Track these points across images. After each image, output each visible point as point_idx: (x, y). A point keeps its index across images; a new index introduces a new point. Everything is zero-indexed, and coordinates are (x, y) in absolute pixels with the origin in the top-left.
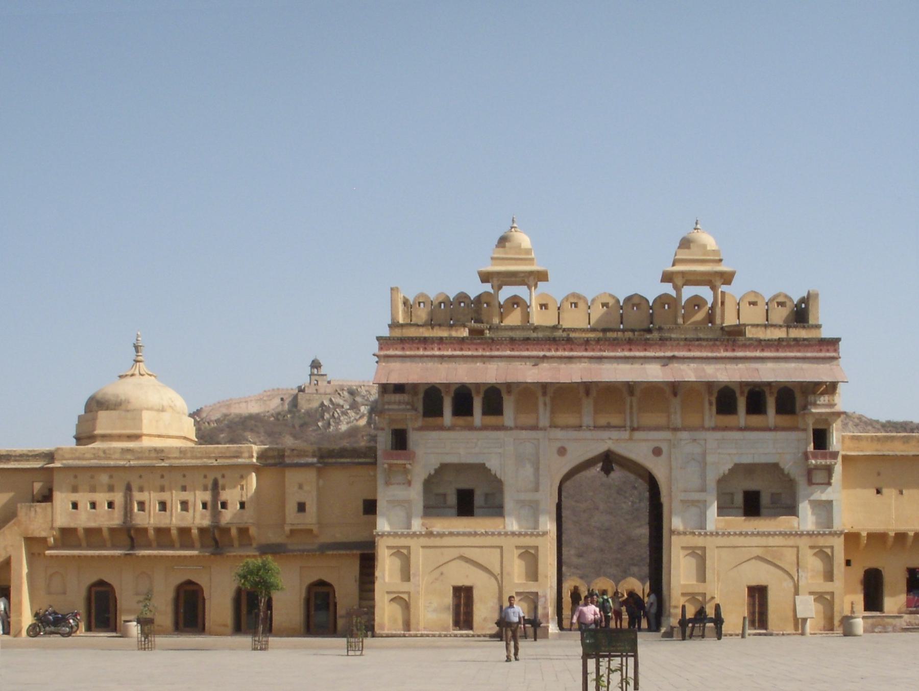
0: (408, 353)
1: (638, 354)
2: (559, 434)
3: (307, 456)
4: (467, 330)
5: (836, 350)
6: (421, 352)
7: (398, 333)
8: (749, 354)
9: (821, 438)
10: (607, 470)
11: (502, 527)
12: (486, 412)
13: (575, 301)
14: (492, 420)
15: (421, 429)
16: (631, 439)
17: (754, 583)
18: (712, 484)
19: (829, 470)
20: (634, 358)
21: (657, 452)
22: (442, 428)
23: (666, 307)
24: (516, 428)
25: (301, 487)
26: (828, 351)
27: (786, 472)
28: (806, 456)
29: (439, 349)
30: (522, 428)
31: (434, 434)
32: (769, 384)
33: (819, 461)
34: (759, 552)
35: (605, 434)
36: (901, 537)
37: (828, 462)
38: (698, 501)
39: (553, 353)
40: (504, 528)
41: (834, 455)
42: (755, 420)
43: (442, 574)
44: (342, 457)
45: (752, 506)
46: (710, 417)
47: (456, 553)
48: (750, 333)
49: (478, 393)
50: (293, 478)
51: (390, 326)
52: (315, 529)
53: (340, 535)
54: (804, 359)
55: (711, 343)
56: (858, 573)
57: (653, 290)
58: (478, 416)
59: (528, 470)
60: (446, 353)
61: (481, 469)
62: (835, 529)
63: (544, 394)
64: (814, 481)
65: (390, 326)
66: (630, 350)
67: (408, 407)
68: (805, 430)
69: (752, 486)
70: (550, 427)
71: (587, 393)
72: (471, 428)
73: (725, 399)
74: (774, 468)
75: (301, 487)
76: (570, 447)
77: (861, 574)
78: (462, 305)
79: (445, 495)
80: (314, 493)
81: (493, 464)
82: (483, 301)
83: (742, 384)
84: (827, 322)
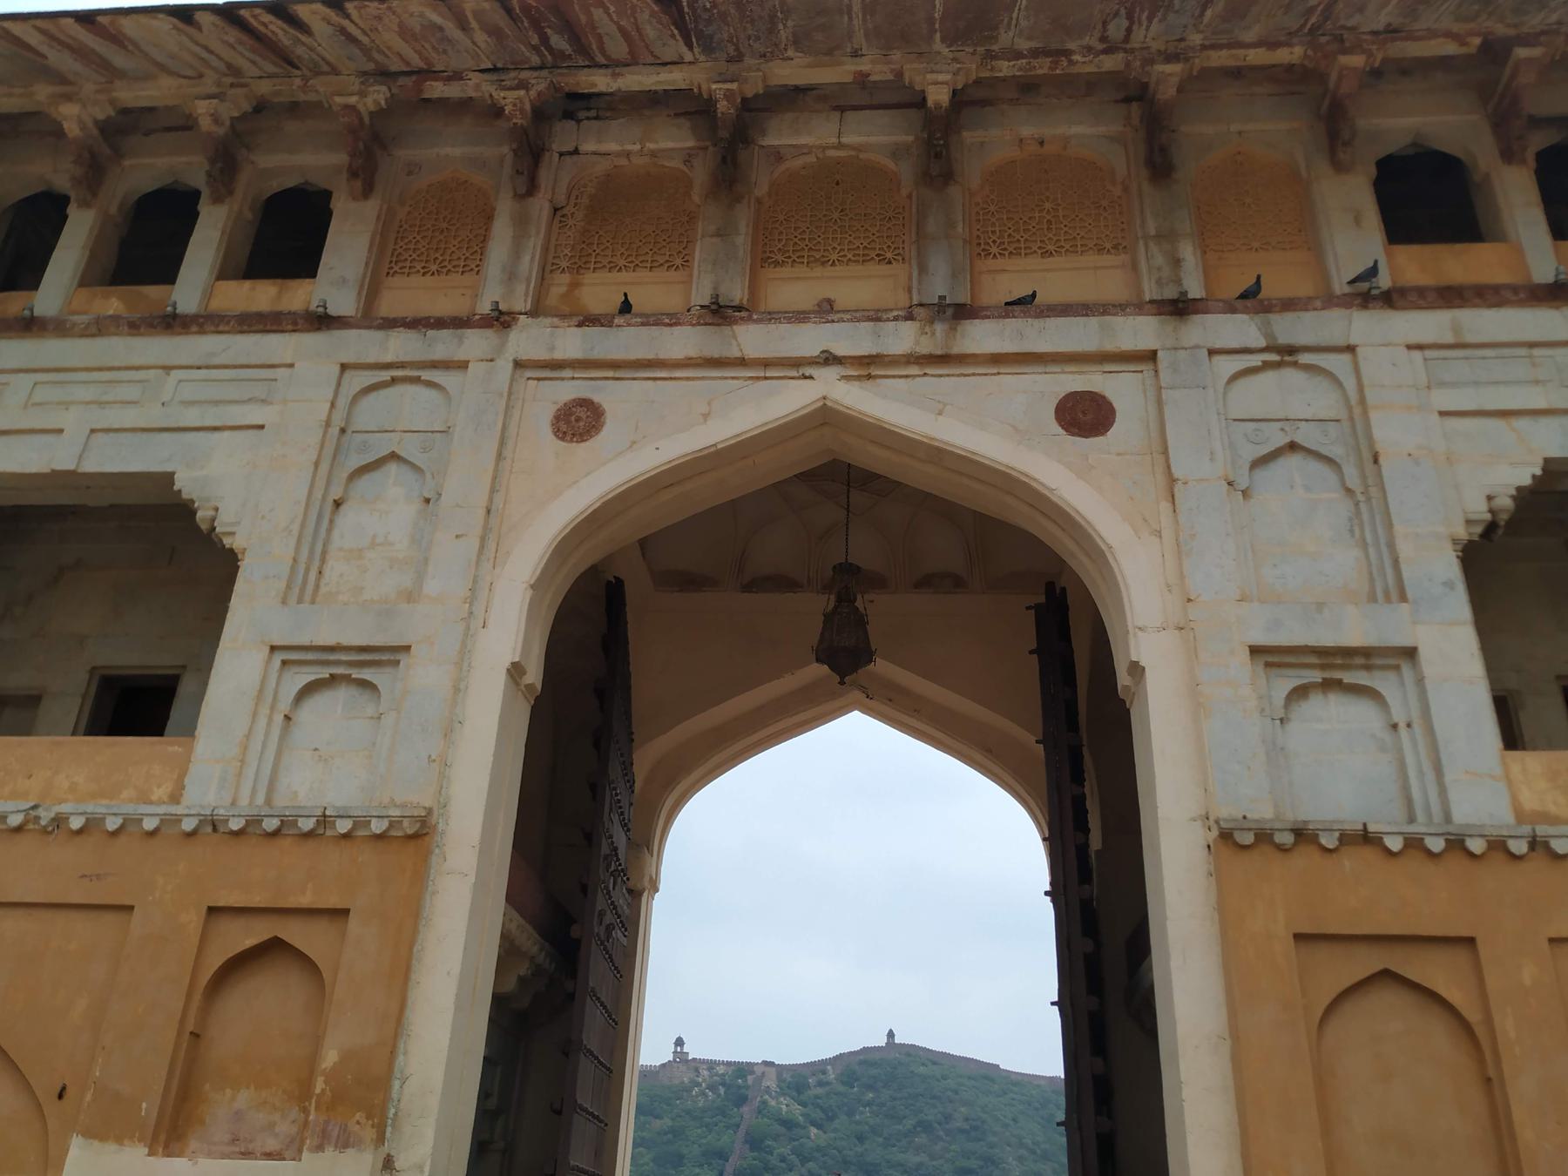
11: (160, 793)
21: (1085, 416)
38: (1365, 656)
40: (175, 798)
58: (191, 286)
70: (534, 313)
76: (613, 396)
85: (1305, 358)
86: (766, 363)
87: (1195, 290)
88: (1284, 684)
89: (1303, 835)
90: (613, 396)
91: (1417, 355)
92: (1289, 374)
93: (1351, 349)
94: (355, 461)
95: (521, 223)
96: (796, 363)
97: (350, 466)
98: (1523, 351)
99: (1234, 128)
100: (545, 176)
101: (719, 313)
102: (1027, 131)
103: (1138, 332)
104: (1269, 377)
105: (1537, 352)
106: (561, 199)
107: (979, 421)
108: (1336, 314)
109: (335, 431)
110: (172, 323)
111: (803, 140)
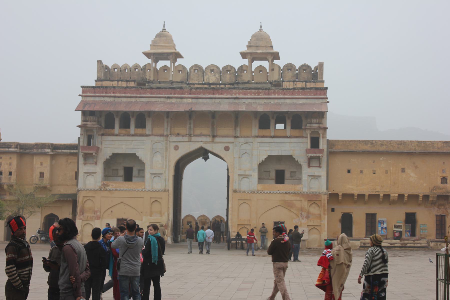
0: (97, 95)
1: (217, 96)
2: (174, 138)
3: (45, 149)
4: (136, 83)
5: (325, 94)
6: (104, 95)
7: (100, 84)
8: (277, 96)
9: (315, 143)
10: (206, 158)
11: (144, 187)
12: (137, 127)
13: (197, 68)
14: (140, 131)
15: (103, 135)
16: (213, 142)
17: (277, 220)
18: (256, 167)
19: (319, 159)
20: (215, 98)
21: (227, 149)
22: (114, 135)
23: (245, 72)
24: (153, 135)
25: (42, 164)
26: (320, 95)
27: (296, 160)
28: (307, 151)
29: (114, 93)
30: (155, 136)
31: (110, 138)
32: (287, 113)
33: (312, 155)
35: (200, 139)
36: (362, 196)
37: (318, 155)
38: (249, 175)
39: (173, 96)
41: (322, 151)
43: (112, 212)
44: (65, 149)
45: (280, 178)
46: (256, 131)
48: (286, 85)
49: (133, 117)
50: (37, 161)
51: (96, 81)
52: (49, 187)
53: (63, 190)
54: (307, 99)
55: (257, 91)
56: (338, 215)
57: (238, 62)
58: (133, 130)
59: (158, 158)
60: (117, 95)
61: (133, 157)
62: (322, 191)
63: (168, 117)
64: (311, 166)
65: (96, 81)
66: (214, 94)
67: (95, 123)
68: (307, 137)
69: (280, 167)
70: (170, 135)
71: (190, 117)
72: (129, 135)
73: (265, 121)
74: (290, 158)
75: (42, 164)
77: (340, 217)
78: (137, 70)
79: (117, 170)
80: (49, 168)
81: (140, 154)
82: (147, 68)
83: (275, 113)
84: (329, 79)
87: (239, 135)
88: (242, 177)
89: (240, 192)
95: (168, 122)
97: (154, 153)
101: (190, 136)
103: (232, 140)
107: (218, 148)
108: (252, 138)
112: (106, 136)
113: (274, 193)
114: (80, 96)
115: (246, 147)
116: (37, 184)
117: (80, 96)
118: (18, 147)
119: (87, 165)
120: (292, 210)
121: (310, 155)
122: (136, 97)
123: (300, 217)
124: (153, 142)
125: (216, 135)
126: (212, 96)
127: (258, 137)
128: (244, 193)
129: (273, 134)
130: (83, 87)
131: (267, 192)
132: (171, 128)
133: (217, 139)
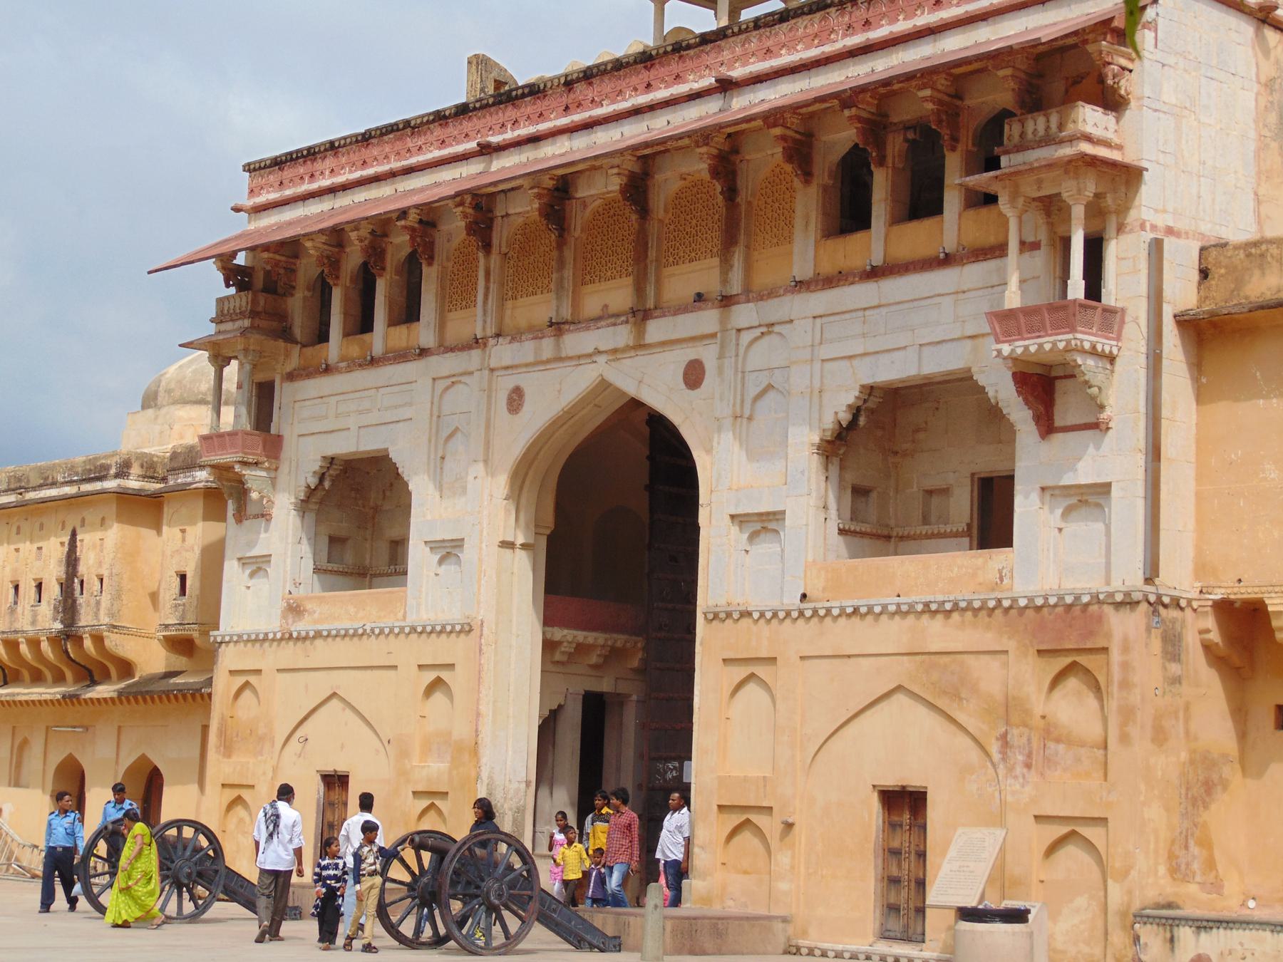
11: (400, 615)
14: (400, 336)
15: (291, 377)
16: (640, 346)
34: (900, 671)
39: (510, 135)
42: (917, 238)
46: (805, 251)
47: (322, 684)
64: (1058, 422)
70: (498, 335)
76: (530, 382)
85: (777, 329)
86: (579, 357)
90: (530, 382)
91: (818, 320)
92: (773, 336)
93: (791, 321)
94: (445, 434)
96: (590, 355)
98: (860, 314)
99: (769, 152)
100: (495, 242)
101: (558, 327)
102: (684, 170)
104: (766, 339)
105: (867, 313)
106: (504, 250)
109: (435, 418)
110: (373, 362)
111: (593, 192)
112: (309, 375)
113: (870, 610)
114: (237, 209)
115: (762, 354)
116: (167, 626)
117: (237, 209)
118: (136, 470)
119: (246, 523)
120: (961, 717)
121: (1019, 347)
122: (392, 175)
123: (996, 756)
124: (441, 385)
125: (650, 304)
126: (642, 99)
127: (801, 286)
128: (746, 622)
129: (877, 259)
130: (250, 168)
131: (842, 609)
132: (502, 300)
133: (656, 330)
